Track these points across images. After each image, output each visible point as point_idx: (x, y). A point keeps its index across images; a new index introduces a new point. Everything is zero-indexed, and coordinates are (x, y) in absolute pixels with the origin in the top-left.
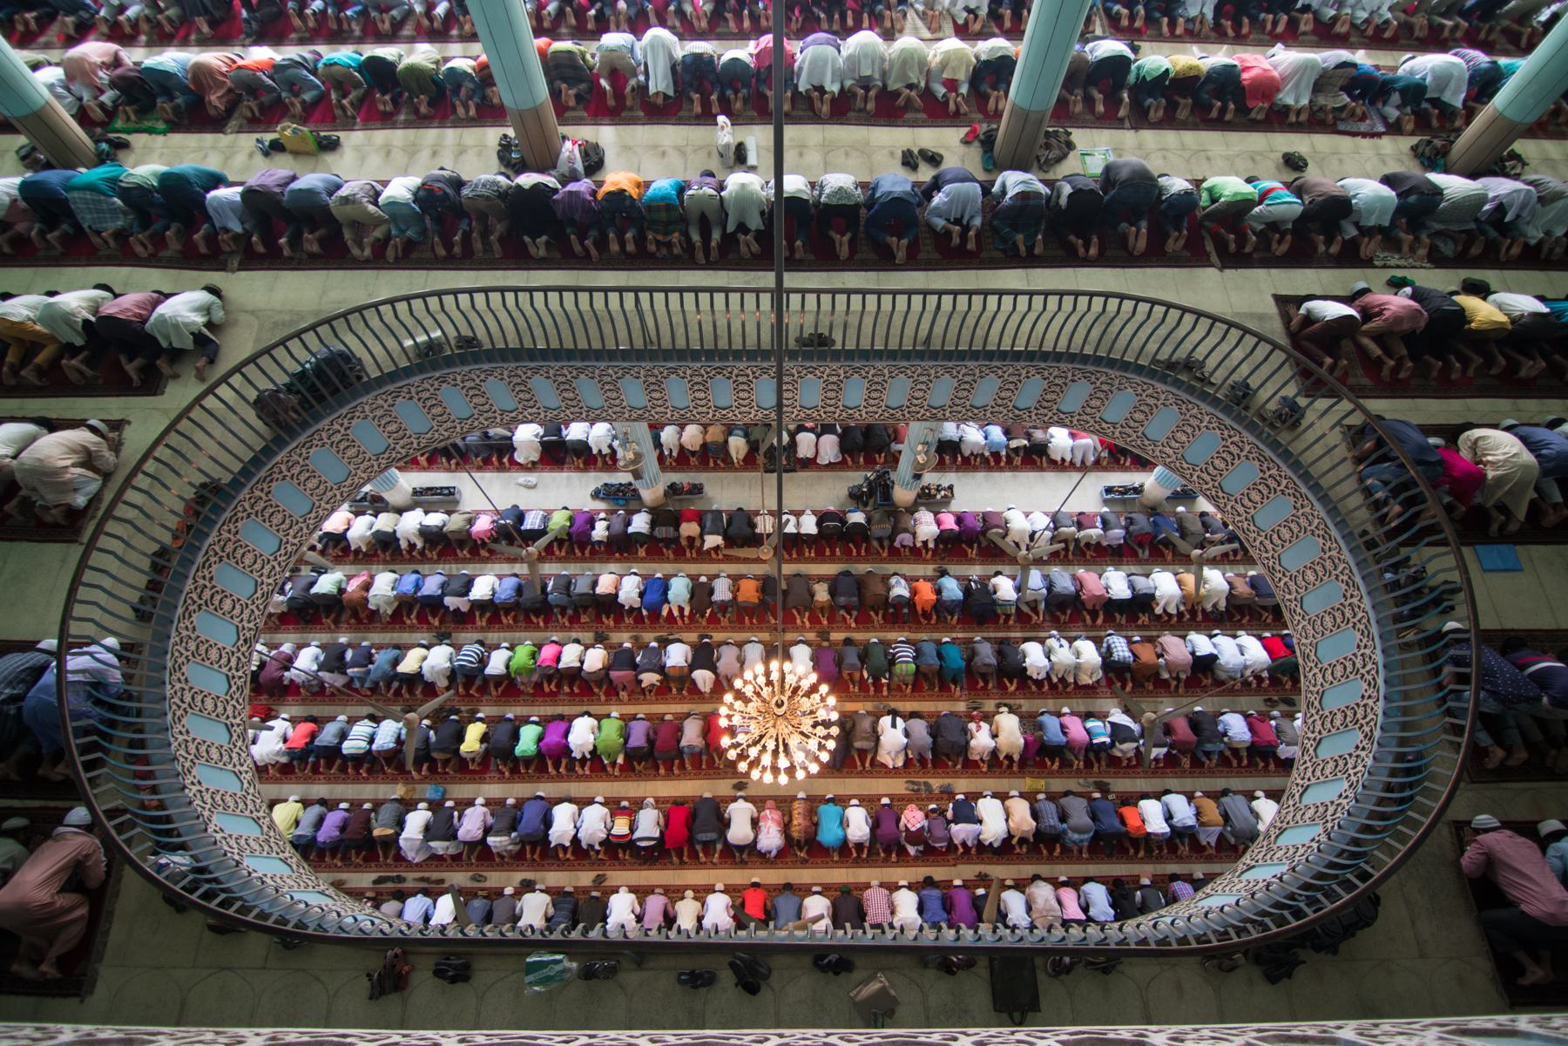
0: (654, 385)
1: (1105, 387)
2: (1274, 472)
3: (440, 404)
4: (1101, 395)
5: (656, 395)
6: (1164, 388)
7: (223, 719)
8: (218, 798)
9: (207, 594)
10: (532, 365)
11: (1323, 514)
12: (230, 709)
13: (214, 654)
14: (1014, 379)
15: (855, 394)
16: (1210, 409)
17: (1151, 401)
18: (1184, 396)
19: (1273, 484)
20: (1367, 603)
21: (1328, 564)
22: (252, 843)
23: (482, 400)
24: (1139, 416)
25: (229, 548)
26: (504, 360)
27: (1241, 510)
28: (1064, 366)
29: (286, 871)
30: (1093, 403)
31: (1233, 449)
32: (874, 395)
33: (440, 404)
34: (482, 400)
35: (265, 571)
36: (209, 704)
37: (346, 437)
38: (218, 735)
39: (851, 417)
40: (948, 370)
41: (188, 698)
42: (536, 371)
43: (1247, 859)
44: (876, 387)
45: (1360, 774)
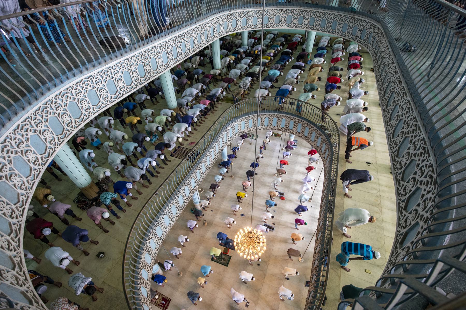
13: (279, 123)
36: (271, 122)
37: (318, 137)
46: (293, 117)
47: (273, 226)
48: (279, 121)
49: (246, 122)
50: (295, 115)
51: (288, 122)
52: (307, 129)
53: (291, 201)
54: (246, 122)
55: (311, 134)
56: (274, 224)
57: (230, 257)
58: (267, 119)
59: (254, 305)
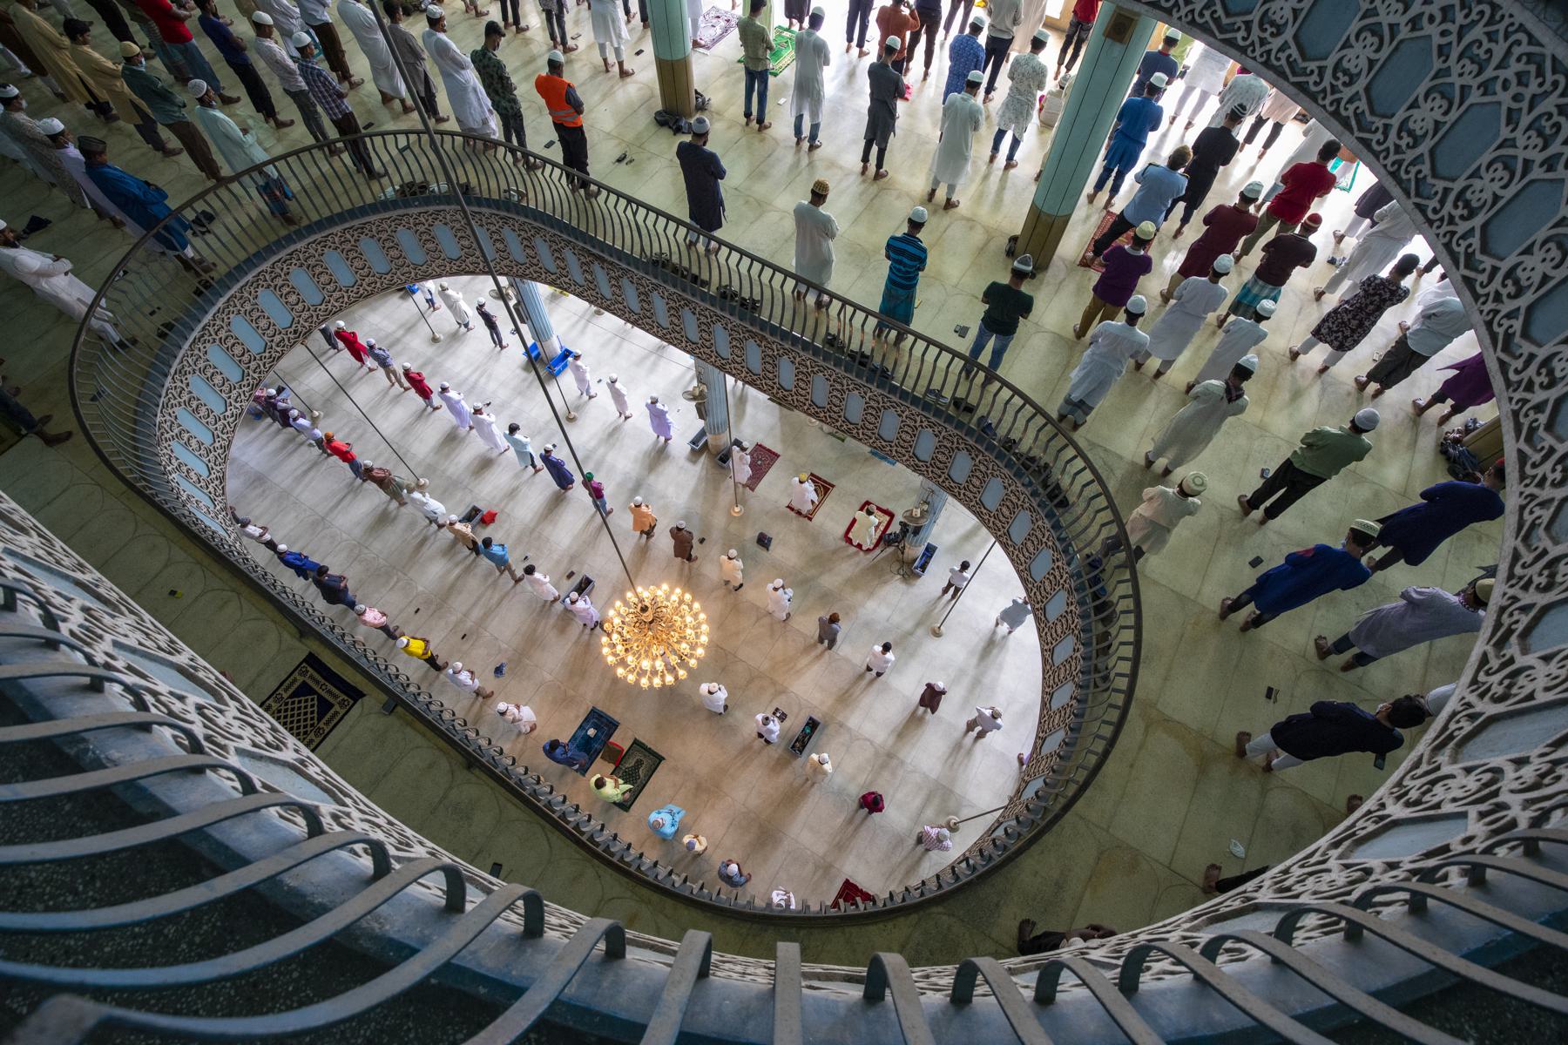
3: (502, 241)
7: (244, 366)
8: (194, 404)
9: (279, 282)
12: (253, 365)
13: (263, 323)
22: (193, 442)
25: (312, 262)
29: (205, 473)
30: (974, 480)
33: (502, 241)
35: (337, 294)
36: (238, 350)
37: (428, 232)
38: (234, 375)
41: (222, 334)
46: (283, 254)
47: (576, 580)
48: (255, 316)
49: (179, 436)
50: (289, 240)
51: (285, 292)
52: (369, 247)
53: (512, 494)
54: (179, 436)
55: (396, 246)
56: (571, 575)
57: (636, 742)
58: (216, 355)
59: (783, 697)
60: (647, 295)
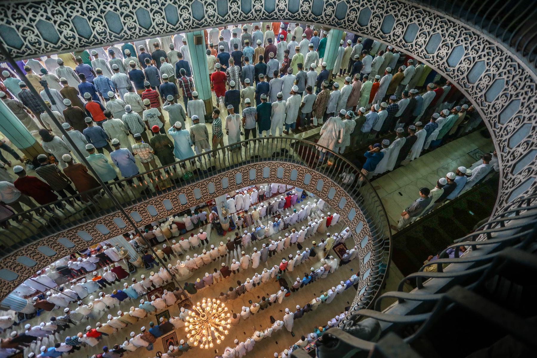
0: (109, 224)
1: (259, 168)
2: (314, 174)
4: (259, 171)
5: (112, 226)
6: (275, 162)
10: (55, 234)
11: (331, 180)
14: (232, 176)
15: (183, 199)
16: (290, 163)
17: (274, 167)
18: (282, 162)
19: (316, 177)
20: (352, 200)
21: (339, 193)
23: (39, 256)
24: (273, 173)
26: (41, 237)
27: (312, 188)
28: (244, 166)
30: (259, 174)
31: (301, 172)
32: (190, 197)
34: (39, 256)
39: (186, 207)
40: (210, 180)
42: (58, 236)
43: (359, 290)
44: (189, 194)
45: (372, 247)
60: (111, 222)
